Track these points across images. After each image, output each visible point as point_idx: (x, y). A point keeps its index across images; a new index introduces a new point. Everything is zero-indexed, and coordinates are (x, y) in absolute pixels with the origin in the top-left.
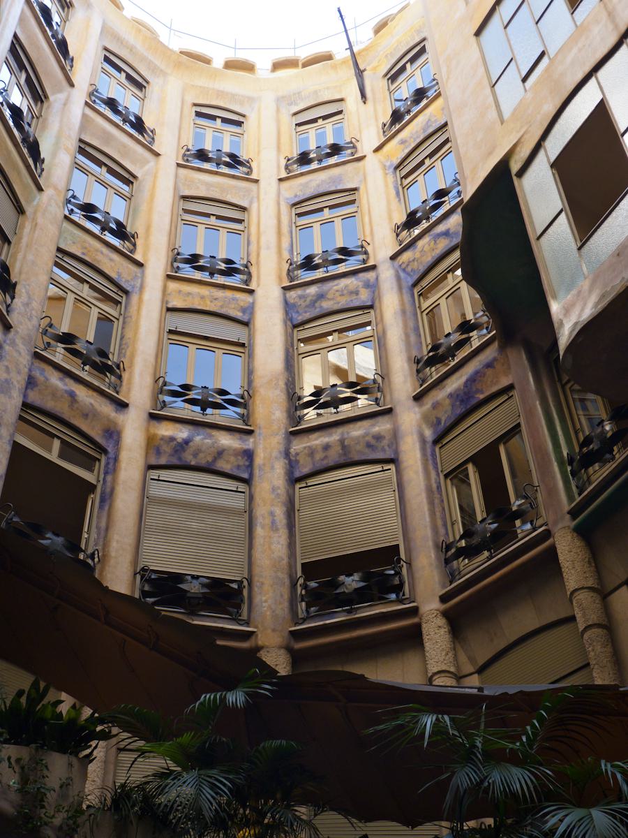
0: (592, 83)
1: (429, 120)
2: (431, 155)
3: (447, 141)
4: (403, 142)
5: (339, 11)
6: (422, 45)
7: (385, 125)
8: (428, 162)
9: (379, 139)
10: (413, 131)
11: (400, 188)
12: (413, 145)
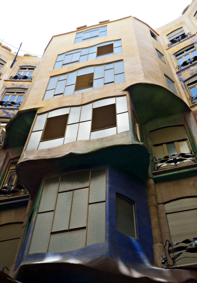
0: (69, 109)
1: (23, 85)
2: (17, 93)
3: (24, 93)
4: (13, 84)
5: (21, 43)
6: (34, 68)
7: (12, 77)
8: (15, 93)
9: (8, 78)
10: (18, 84)
11: (4, 94)
12: (15, 87)
